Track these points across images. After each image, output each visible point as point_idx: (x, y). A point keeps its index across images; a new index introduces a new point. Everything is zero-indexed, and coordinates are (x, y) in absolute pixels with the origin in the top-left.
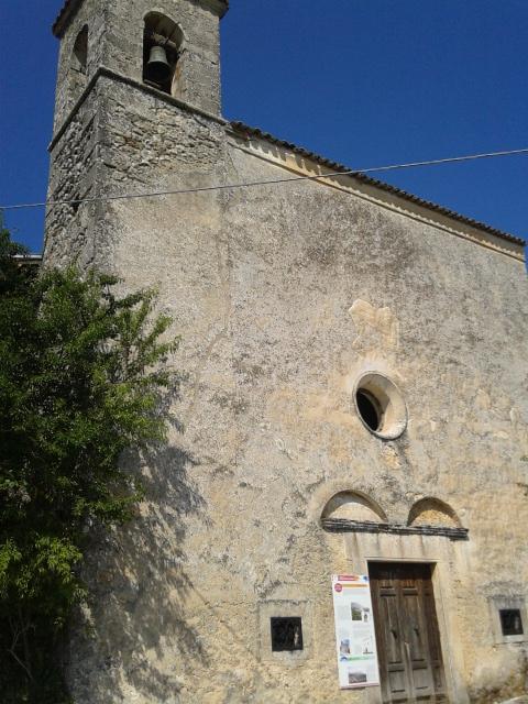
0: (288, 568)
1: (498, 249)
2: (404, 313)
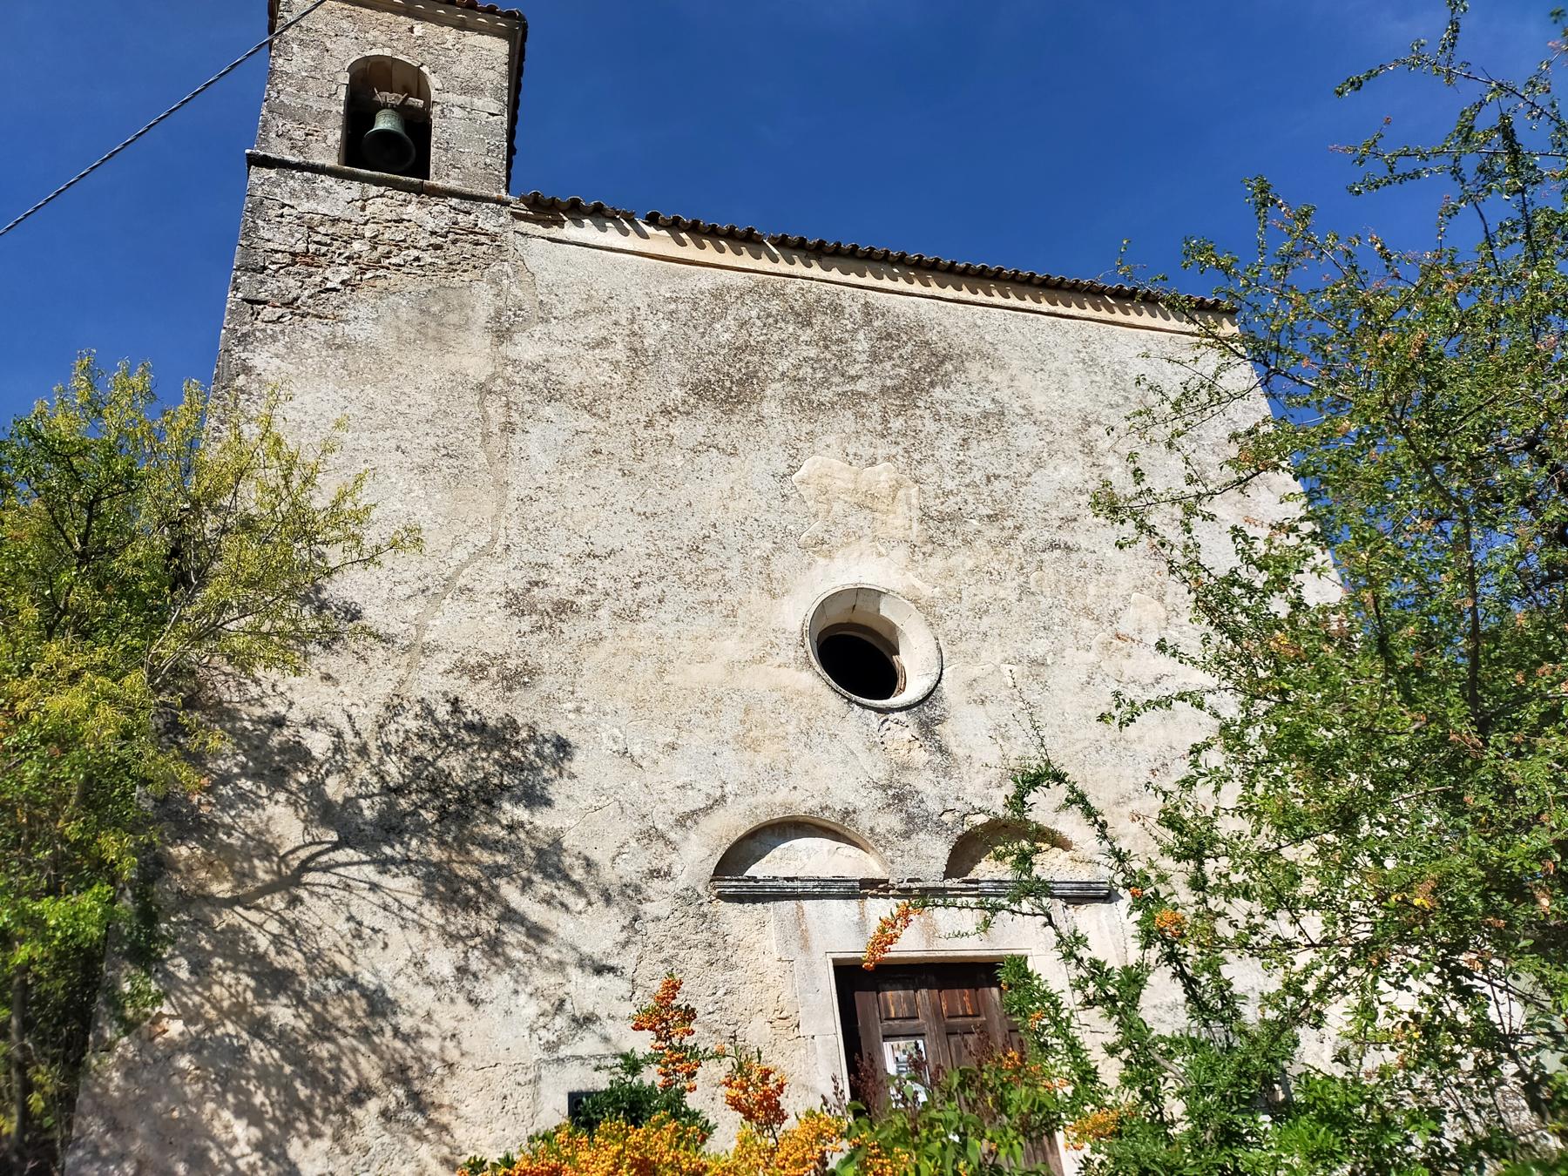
2: (928, 469)
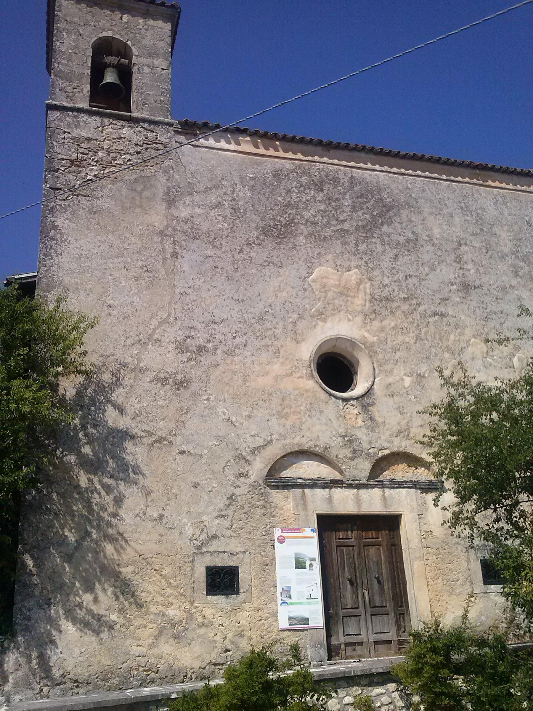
0: (226, 523)
1: (510, 186)
2: (376, 272)
